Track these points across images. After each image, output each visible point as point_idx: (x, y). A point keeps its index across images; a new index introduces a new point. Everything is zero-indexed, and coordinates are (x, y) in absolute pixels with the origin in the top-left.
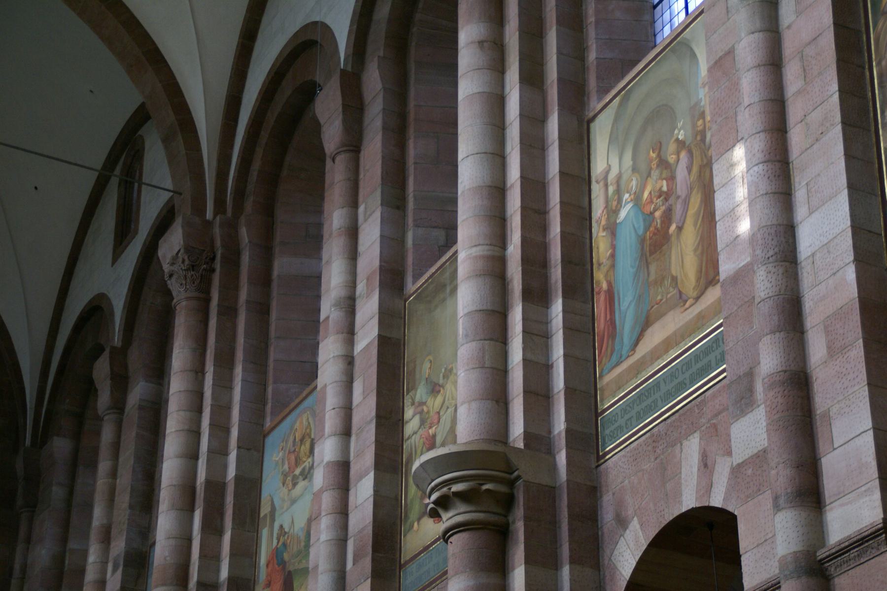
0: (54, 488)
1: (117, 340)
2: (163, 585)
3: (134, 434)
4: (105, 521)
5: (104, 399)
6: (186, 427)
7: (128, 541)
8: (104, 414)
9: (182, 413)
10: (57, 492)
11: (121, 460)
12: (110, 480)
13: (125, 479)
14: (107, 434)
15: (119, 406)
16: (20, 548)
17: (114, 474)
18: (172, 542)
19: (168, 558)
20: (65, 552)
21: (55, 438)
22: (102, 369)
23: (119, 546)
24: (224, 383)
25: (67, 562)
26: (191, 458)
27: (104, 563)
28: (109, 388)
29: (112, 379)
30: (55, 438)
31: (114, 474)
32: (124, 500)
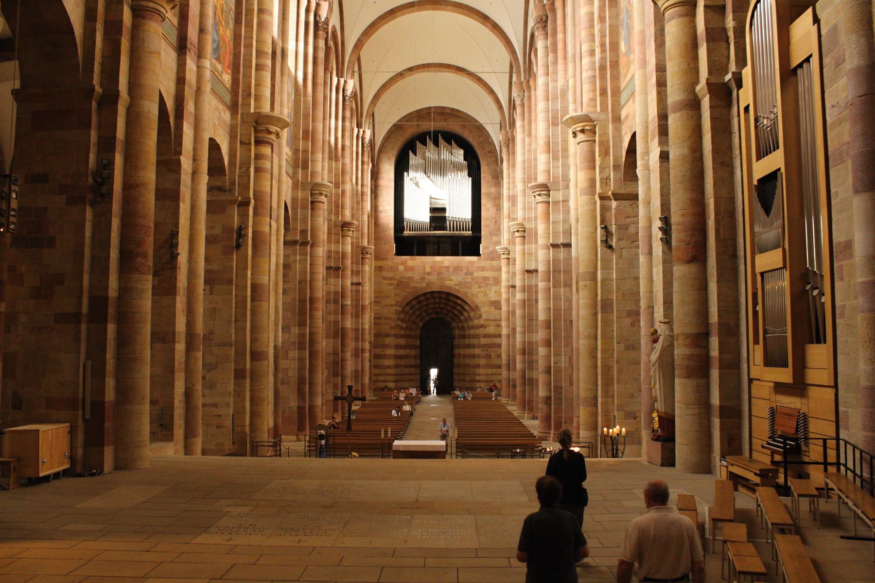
24: (514, 172)
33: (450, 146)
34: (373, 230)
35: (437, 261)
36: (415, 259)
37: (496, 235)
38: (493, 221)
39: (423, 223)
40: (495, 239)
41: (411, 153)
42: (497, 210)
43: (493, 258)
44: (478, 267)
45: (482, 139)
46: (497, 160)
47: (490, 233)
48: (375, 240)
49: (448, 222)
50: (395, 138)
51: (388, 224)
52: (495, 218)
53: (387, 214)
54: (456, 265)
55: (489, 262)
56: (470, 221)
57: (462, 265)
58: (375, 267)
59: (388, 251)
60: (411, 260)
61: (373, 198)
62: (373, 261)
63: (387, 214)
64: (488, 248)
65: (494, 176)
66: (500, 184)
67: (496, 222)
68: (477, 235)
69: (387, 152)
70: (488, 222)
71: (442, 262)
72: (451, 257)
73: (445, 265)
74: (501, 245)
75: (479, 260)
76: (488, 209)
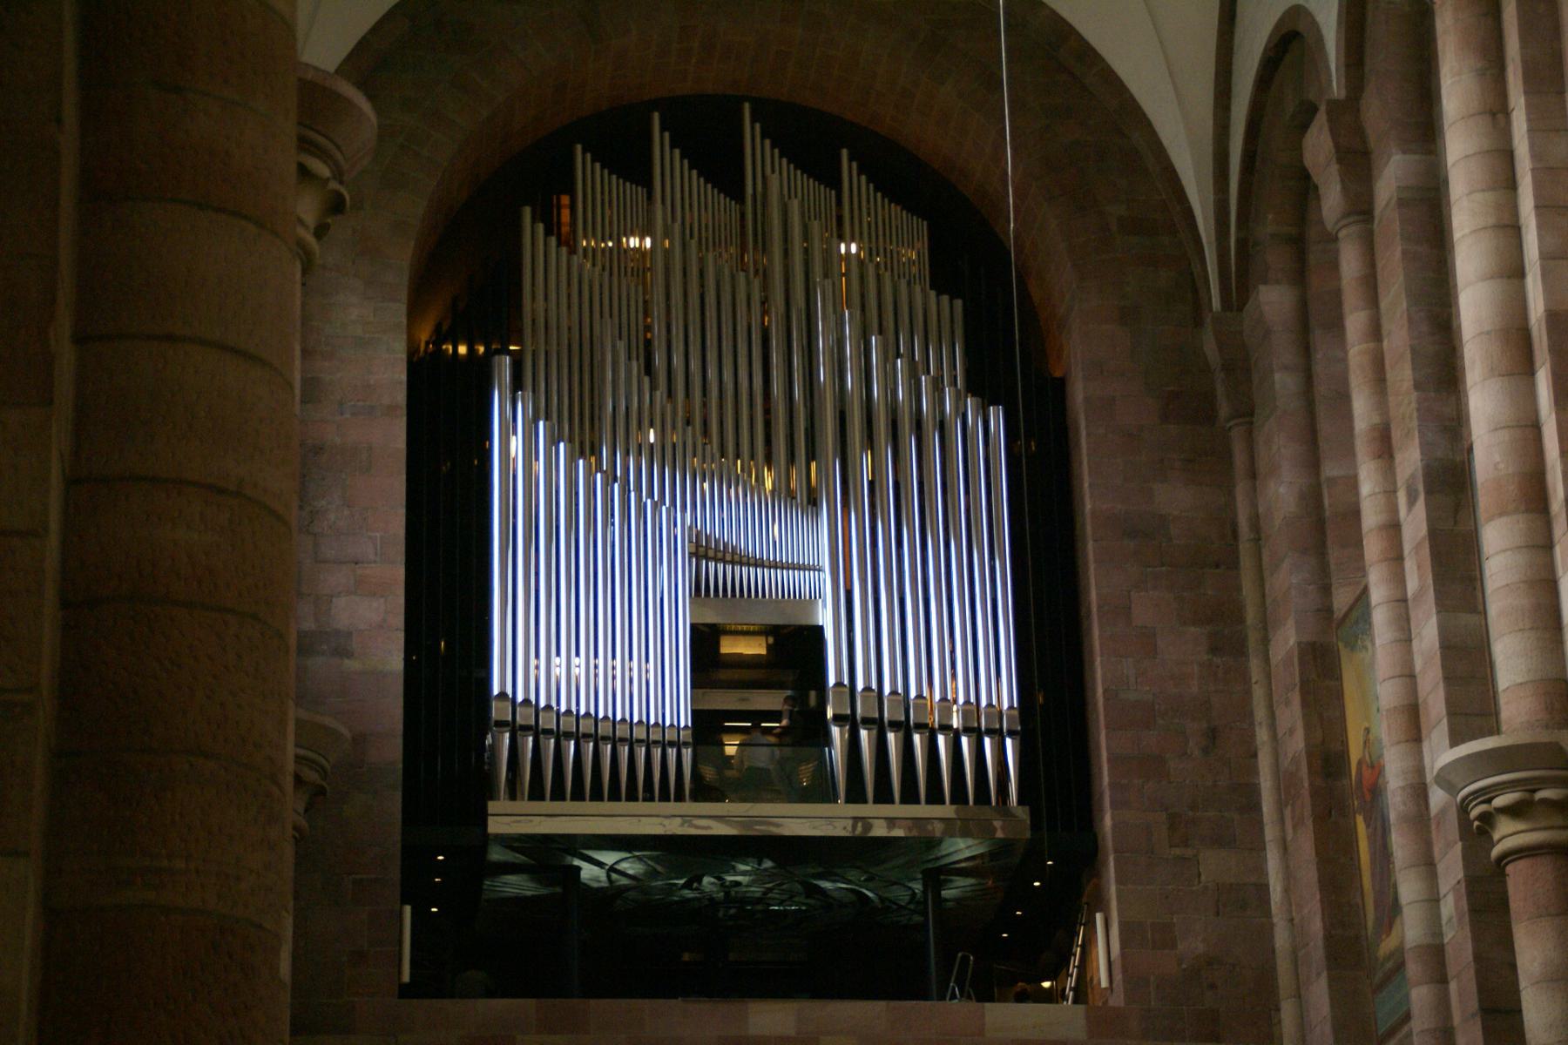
0: (1277, 376)
1: (1337, 87)
2: (1501, 514)
3: (1398, 254)
4: (1376, 420)
5: (1332, 199)
6: (1491, 221)
7: (1425, 447)
8: (1337, 227)
9: (1479, 196)
10: (1284, 383)
11: (1383, 305)
12: (1372, 345)
13: (1398, 338)
14: (1350, 263)
15: (1361, 208)
16: (1241, 489)
17: (1375, 332)
18: (1504, 435)
19: (1502, 466)
20: (1319, 485)
21: (1262, 288)
22: (1318, 146)
23: (1410, 459)
25: (1326, 502)
26: (1509, 277)
27: (1391, 493)
28: (1338, 178)
29: (1340, 161)
30: (1262, 288)
31: (1375, 332)
32: (1402, 376)
39: (657, 739)
40: (1215, 865)
42: (1214, 650)
51: (360, 740)
53: (352, 665)
63: (352, 665)
64: (1174, 947)
66: (1227, 456)
67: (1213, 734)
72: (880, 1006)
74: (1495, 730)
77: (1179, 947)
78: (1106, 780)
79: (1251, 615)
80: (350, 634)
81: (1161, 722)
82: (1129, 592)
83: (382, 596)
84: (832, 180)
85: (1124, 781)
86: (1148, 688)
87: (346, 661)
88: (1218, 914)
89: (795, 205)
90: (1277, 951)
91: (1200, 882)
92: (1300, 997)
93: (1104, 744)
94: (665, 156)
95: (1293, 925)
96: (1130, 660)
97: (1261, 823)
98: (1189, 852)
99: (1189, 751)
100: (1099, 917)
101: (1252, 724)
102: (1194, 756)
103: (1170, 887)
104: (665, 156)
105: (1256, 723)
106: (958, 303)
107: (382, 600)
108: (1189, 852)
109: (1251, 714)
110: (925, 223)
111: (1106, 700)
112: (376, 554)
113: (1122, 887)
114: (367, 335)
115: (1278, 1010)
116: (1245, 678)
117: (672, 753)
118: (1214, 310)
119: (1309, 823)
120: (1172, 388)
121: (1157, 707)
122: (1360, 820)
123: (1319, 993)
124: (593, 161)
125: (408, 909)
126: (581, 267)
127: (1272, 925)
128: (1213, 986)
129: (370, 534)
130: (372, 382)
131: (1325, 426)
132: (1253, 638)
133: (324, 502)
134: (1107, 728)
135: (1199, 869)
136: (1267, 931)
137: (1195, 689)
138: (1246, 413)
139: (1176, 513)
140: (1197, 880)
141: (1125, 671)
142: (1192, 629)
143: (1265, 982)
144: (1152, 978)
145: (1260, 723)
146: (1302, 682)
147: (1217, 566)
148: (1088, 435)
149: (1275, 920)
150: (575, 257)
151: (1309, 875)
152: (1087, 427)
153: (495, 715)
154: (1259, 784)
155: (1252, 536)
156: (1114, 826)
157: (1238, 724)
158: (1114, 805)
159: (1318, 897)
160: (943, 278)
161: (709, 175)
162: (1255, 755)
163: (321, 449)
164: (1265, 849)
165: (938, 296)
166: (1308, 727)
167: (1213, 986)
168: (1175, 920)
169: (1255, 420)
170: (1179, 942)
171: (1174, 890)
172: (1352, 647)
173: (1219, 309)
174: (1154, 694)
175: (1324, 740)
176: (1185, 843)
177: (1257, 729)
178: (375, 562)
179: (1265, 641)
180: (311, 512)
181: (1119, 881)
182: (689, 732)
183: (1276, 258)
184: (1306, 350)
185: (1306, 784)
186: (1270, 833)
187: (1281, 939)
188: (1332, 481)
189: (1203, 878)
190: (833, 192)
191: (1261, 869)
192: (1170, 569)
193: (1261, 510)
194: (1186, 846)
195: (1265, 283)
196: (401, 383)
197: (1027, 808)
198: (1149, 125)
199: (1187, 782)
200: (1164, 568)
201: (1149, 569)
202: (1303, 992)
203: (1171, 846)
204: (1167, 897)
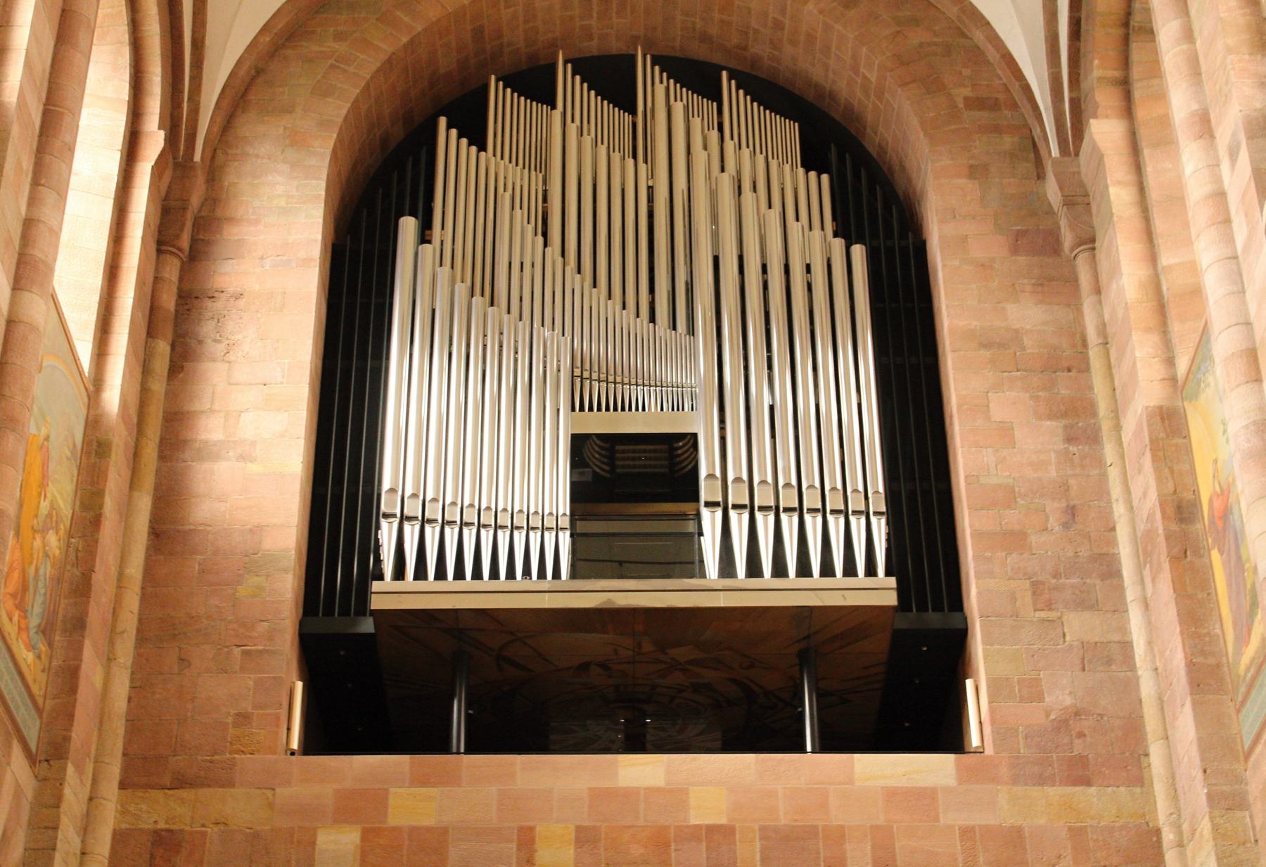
25: (1164, 288)
30: (1092, 121)
33: (709, 106)
34: (135, 568)
35: (628, 796)
36: (452, 779)
37: (1084, 603)
38: (1054, 508)
40: (1079, 626)
41: (447, 138)
42: (1069, 440)
43: (1082, 761)
44: (967, 833)
45: (917, 37)
46: (1033, 149)
47: (1036, 587)
48: (141, 639)
49: (710, 521)
50: (339, 37)
51: (257, 530)
52: (1064, 488)
53: (253, 468)
54: (784, 819)
55: (1055, 792)
56: (878, 503)
57: (837, 816)
58: (119, 838)
59: (243, 718)
60: (421, 781)
61: (161, 365)
62: (110, 790)
64: (1041, 699)
65: (1019, 235)
66: (1073, 281)
67: (1072, 511)
68: (934, 619)
69: (289, 110)
70: (1012, 518)
71: (676, 795)
73: (694, 820)
75: (965, 776)
76: (1006, 433)
77: (1047, 699)
78: (970, 553)
79: (1103, 408)
80: (253, 443)
81: (1022, 502)
82: (987, 392)
83: (286, 411)
84: (716, 96)
85: (988, 554)
86: (1008, 474)
87: (249, 464)
88: (1084, 669)
89: (678, 108)
90: (1143, 700)
91: (1064, 641)
92: (1167, 738)
93: (968, 523)
94: (567, 82)
95: (1157, 674)
96: (990, 450)
97: (1121, 588)
98: (1053, 615)
99: (1049, 529)
100: (969, 683)
101: (1109, 502)
102: (1054, 531)
103: (1036, 646)
104: (567, 82)
105: (1113, 501)
106: (825, 178)
107: (286, 414)
108: (1053, 615)
109: (1108, 494)
110: (796, 124)
111: (968, 484)
112: (283, 377)
113: (988, 647)
114: (290, 205)
115: (1147, 755)
116: (1100, 463)
117: (550, 538)
118: (1053, 155)
119: (1166, 566)
120: (1019, 228)
121: (1017, 489)
122: (1215, 555)
123: (1186, 726)
124: (505, 88)
125: (299, 686)
126: (487, 161)
127: (1137, 678)
128: (1081, 735)
129: (278, 361)
130: (290, 241)
131: (1159, 225)
132: (1106, 426)
133: (239, 337)
134: (969, 509)
135: (1063, 629)
136: (1131, 684)
137: (1053, 474)
138: (1089, 241)
139: (1028, 327)
140: (1062, 640)
141: (985, 459)
142: (1048, 423)
143: (1133, 730)
144: (1021, 729)
145: (1117, 500)
146: (1152, 441)
147: (1069, 370)
148: (944, 266)
149: (1140, 673)
150: (483, 154)
151: (1168, 613)
152: (943, 260)
153: (383, 508)
154: (1119, 554)
155: (1100, 341)
156: (979, 593)
157: (1096, 502)
158: (977, 576)
159: (1178, 630)
160: (812, 160)
161: (604, 93)
162: (1113, 529)
163: (241, 295)
164: (1127, 611)
165: (807, 172)
166: (1160, 480)
167: (1081, 735)
168: (1041, 676)
169: (1097, 244)
170: (1046, 695)
171: (1039, 649)
172: (1195, 396)
173: (1058, 155)
174: (1014, 479)
175: (1175, 491)
176: (1049, 606)
177: (1114, 506)
178: (282, 383)
179: (1118, 427)
180: (228, 345)
181: (984, 643)
182: (567, 519)
183: (1104, 97)
184: (1138, 167)
185: (1161, 531)
186: (1131, 593)
187: (1147, 687)
188: (1170, 268)
189: (1068, 638)
190: (715, 104)
191: (1124, 629)
192: (1024, 373)
193: (1107, 317)
194: (1050, 610)
195: (1095, 116)
196: (316, 241)
197: (892, 582)
198: (988, 23)
199: (1049, 553)
200: (1019, 373)
201: (1005, 374)
202: (1169, 733)
203: (1035, 610)
204: (1033, 656)
